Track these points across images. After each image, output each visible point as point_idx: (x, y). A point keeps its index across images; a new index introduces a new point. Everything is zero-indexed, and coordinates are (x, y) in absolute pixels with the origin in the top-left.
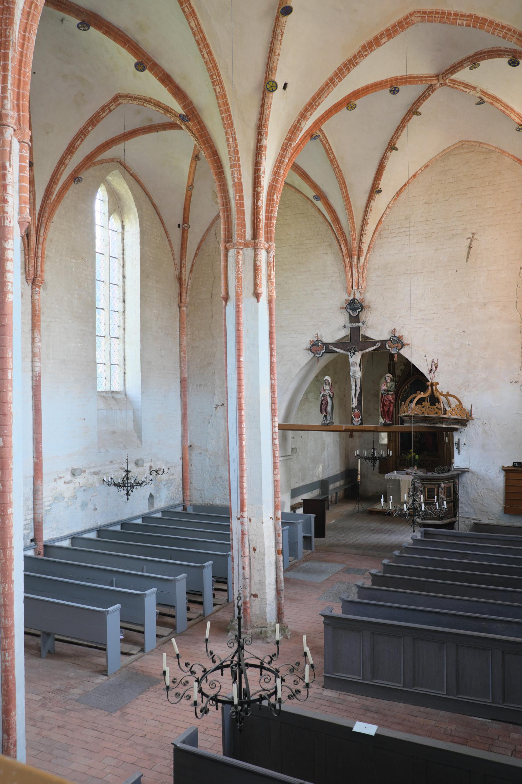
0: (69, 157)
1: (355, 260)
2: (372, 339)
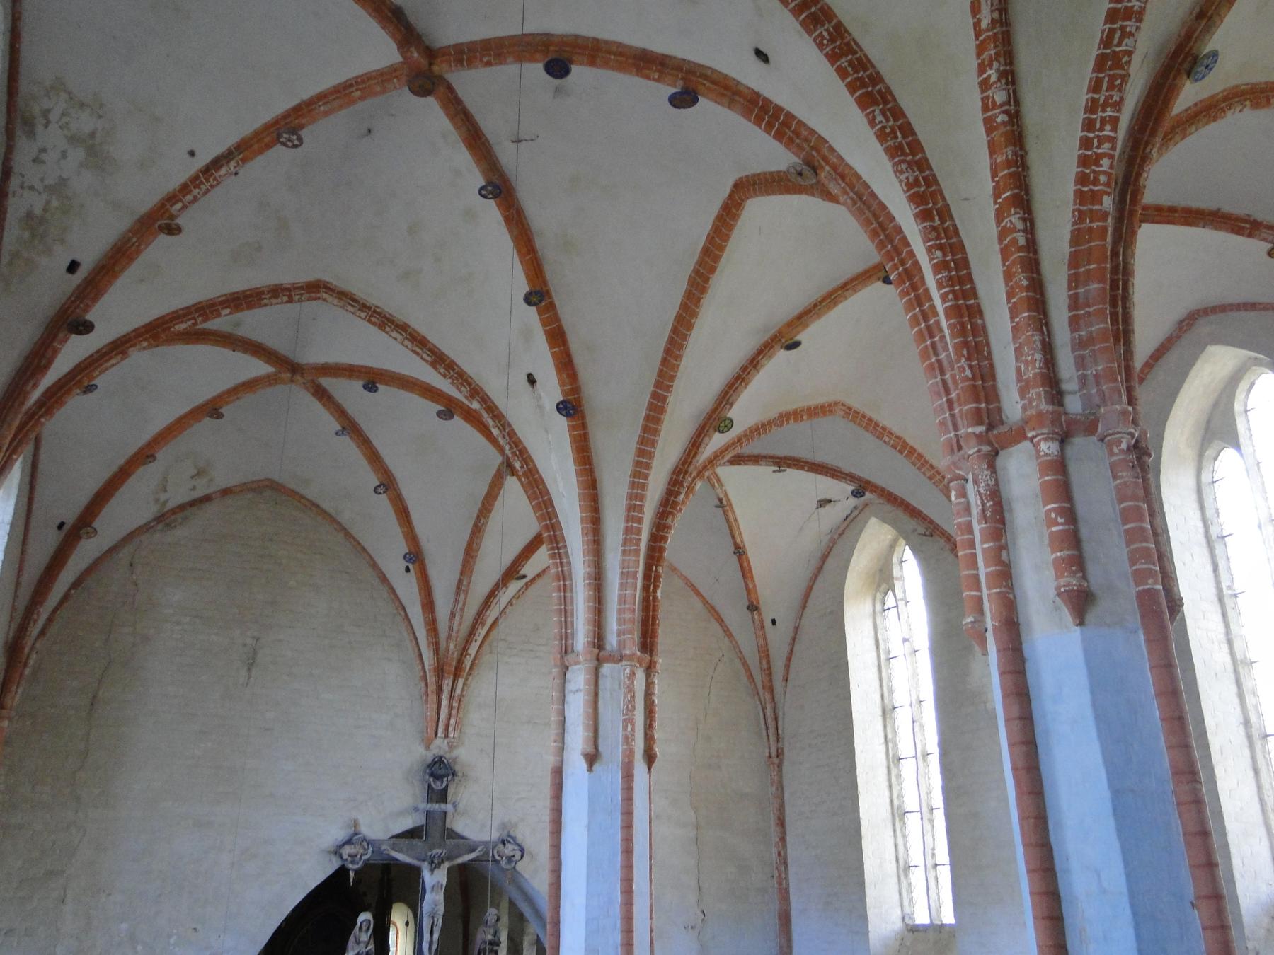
0: (145, 344)
1: (447, 683)
2: (463, 838)
